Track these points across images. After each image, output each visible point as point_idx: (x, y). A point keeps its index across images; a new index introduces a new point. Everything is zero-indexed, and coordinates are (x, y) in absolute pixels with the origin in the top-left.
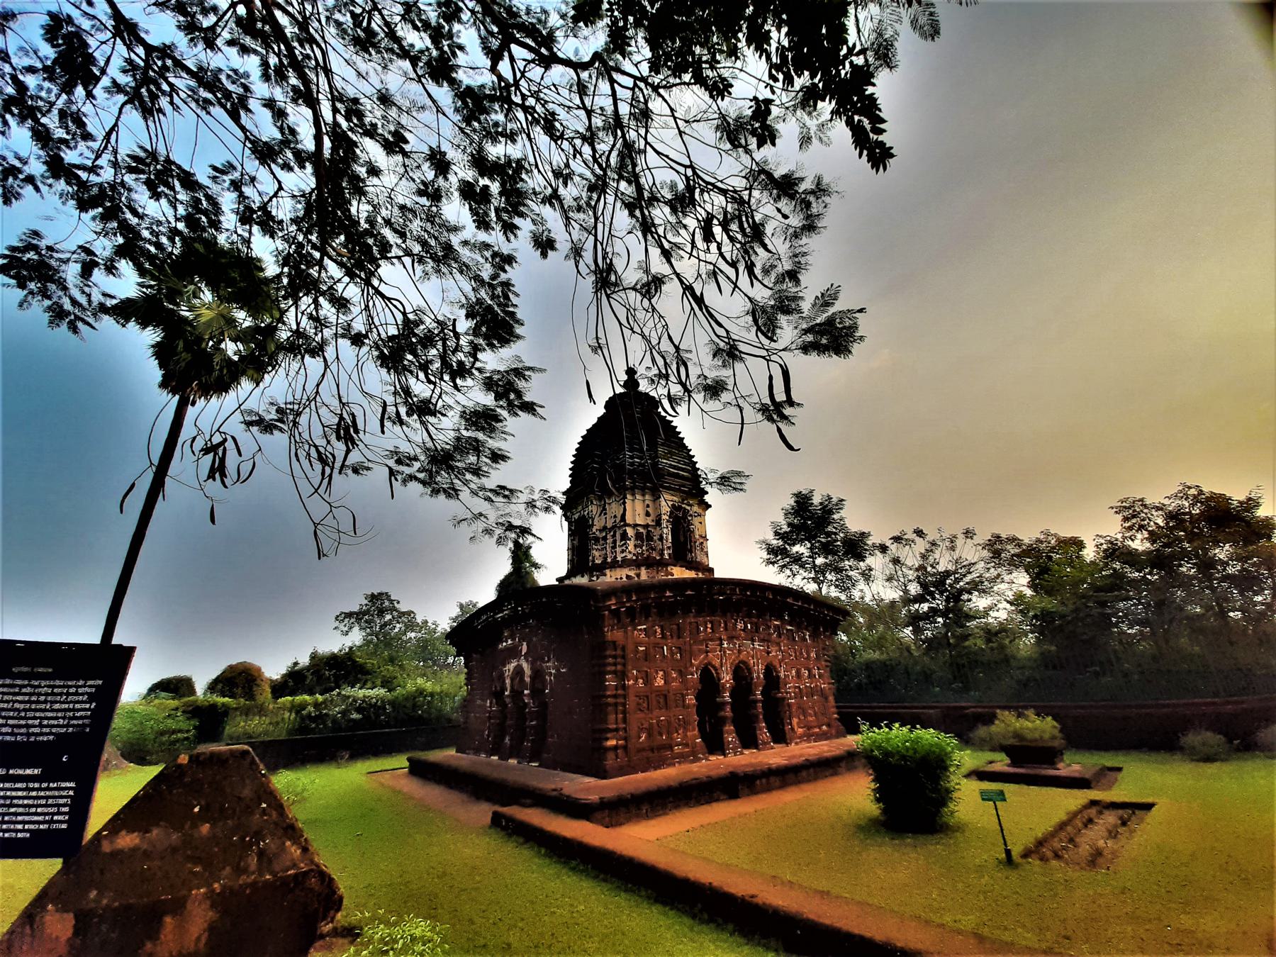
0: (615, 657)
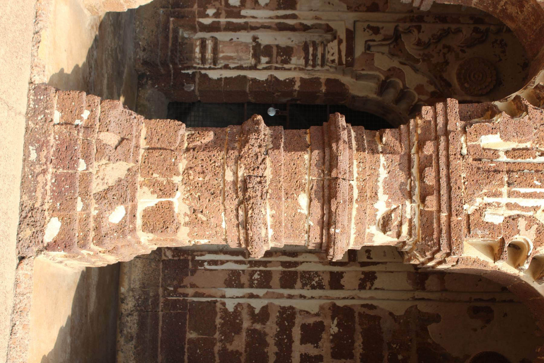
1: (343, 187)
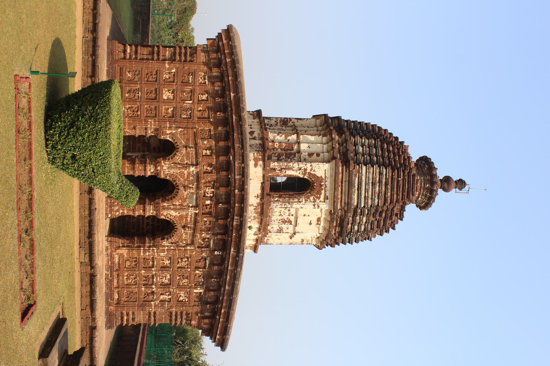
0: (186, 54)
1: (146, 210)
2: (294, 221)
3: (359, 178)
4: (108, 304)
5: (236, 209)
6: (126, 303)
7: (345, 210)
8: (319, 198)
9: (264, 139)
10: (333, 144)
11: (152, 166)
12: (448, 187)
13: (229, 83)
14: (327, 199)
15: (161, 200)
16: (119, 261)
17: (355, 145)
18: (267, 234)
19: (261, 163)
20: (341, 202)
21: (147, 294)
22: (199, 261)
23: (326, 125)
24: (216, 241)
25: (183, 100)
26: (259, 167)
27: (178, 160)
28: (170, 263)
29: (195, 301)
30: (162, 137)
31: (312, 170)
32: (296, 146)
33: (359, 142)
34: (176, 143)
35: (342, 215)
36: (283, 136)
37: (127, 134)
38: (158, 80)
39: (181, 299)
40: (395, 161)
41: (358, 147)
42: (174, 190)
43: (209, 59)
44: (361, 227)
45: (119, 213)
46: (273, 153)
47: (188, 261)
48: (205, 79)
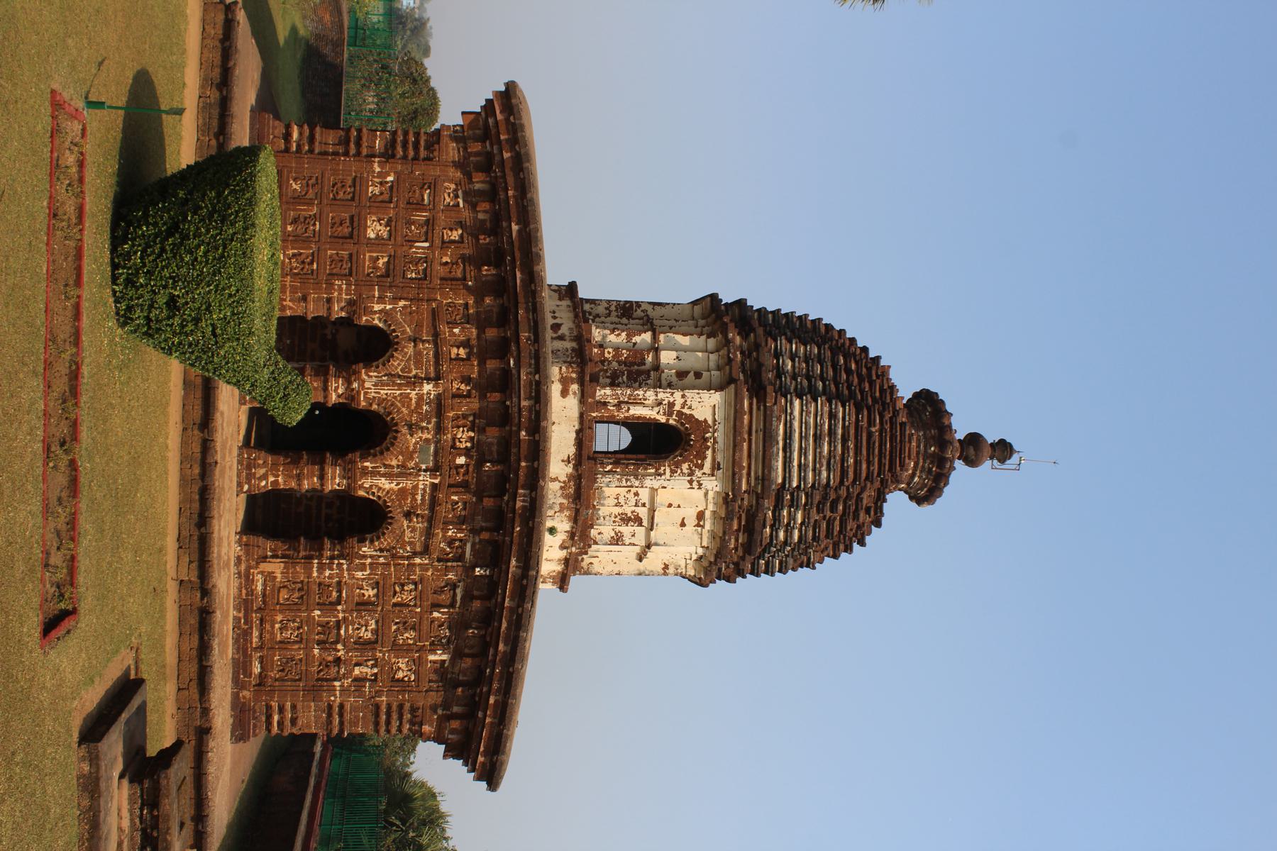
0: (416, 145)
1: (326, 476)
2: (646, 516)
3: (785, 424)
4: (238, 684)
5: (521, 473)
6: (277, 683)
7: (757, 494)
8: (701, 467)
9: (582, 340)
10: (729, 352)
11: (340, 382)
12: (976, 455)
13: (508, 203)
14: (719, 469)
15: (358, 454)
16: (264, 590)
17: (777, 355)
18: (590, 546)
19: (575, 387)
20: (749, 474)
21: (324, 663)
22: (439, 591)
23: (714, 315)
24: (477, 546)
25: (409, 241)
26: (572, 396)
27: (396, 368)
28: (377, 596)
29: (430, 681)
30: (364, 318)
31: (686, 407)
32: (651, 355)
33: (786, 349)
34: (394, 331)
35: (751, 506)
36: (624, 334)
37: (288, 313)
38: (357, 198)
39: (400, 675)
40: (862, 391)
41: (783, 361)
42: (387, 435)
43: (467, 155)
44: (791, 533)
45: (267, 483)
46: (601, 370)
47: (416, 589)
48: (457, 196)
